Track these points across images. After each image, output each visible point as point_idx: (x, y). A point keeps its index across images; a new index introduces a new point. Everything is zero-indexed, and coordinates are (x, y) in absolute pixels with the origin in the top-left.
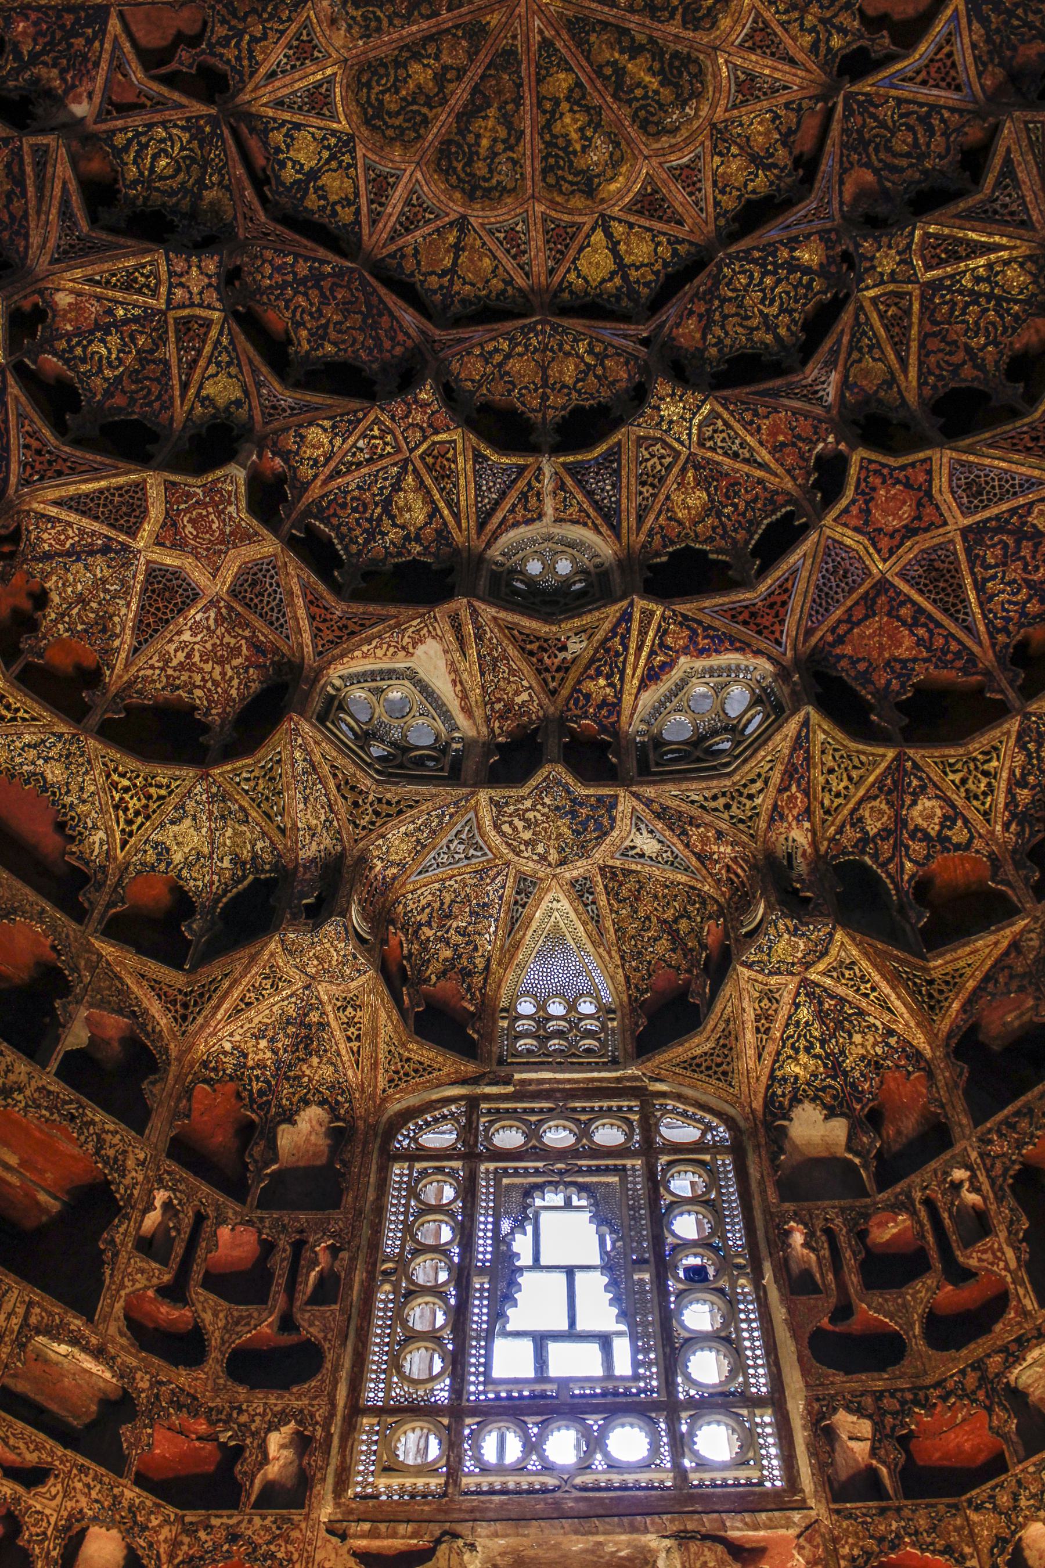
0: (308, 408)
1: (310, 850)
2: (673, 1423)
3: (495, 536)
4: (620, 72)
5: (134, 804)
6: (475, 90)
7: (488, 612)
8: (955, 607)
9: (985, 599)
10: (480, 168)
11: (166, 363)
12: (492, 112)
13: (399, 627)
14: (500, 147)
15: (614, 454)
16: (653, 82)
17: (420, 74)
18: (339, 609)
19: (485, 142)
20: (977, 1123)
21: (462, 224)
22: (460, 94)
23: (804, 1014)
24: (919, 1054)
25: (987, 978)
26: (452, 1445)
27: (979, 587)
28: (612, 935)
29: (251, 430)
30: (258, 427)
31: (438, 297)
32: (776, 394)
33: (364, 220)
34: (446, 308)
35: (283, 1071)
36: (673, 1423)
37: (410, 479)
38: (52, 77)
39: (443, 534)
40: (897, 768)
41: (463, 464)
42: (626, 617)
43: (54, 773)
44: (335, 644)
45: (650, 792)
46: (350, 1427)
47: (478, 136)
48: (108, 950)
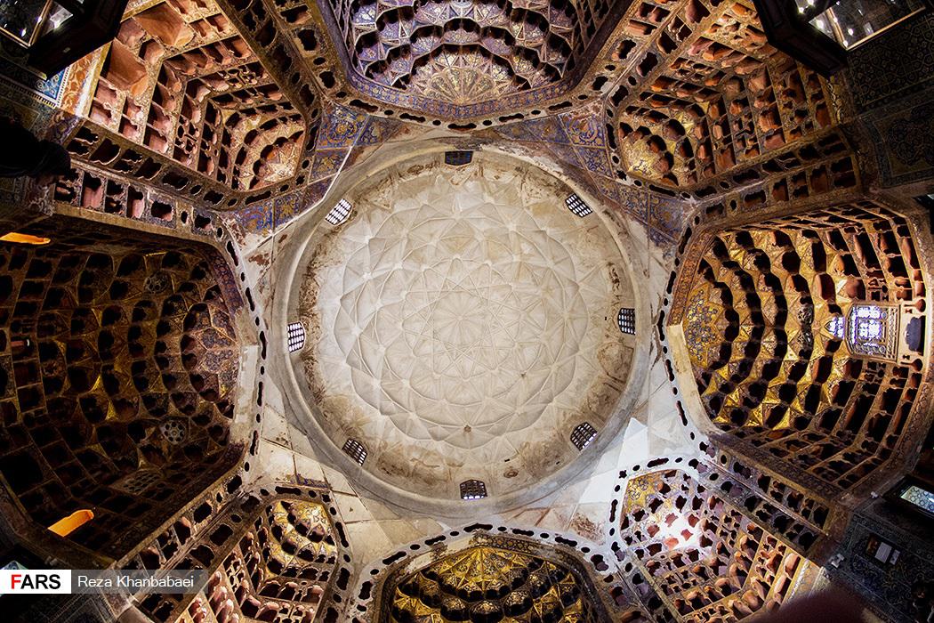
17: (480, 89)
22: (474, 87)
32: (422, 24)
38: (542, 78)
39: (480, 7)
41: (476, 16)
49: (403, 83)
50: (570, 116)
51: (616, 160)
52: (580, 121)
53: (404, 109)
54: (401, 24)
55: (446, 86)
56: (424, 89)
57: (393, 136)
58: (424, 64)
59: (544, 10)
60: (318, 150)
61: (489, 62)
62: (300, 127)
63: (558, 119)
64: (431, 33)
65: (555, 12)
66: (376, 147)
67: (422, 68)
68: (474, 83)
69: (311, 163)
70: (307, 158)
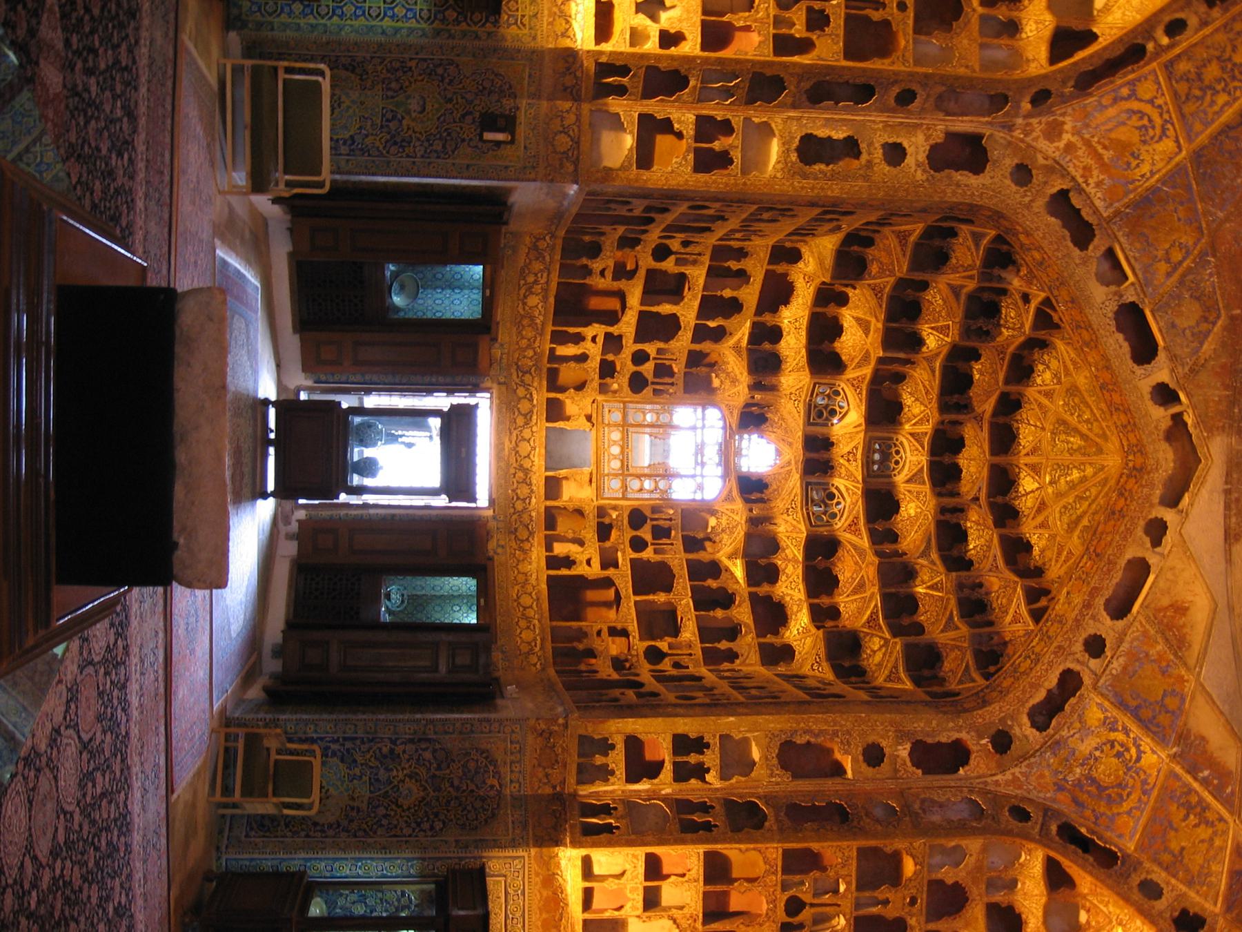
0: (933, 371)
1: (783, 380)
2: (621, 475)
3: (907, 439)
4: (1086, 499)
5: (797, 324)
6: (1087, 436)
7: (862, 435)
8: (855, 592)
9: (852, 601)
10: (1063, 437)
11: (938, 322)
12: (1083, 443)
13: (859, 406)
14: (1070, 445)
15: (924, 483)
16: (1078, 512)
18: (864, 387)
19: (1072, 439)
20: (687, 560)
21: (1043, 429)
22: (1084, 428)
23: (735, 524)
24: (718, 552)
25: (732, 574)
26: (616, 425)
27: (855, 600)
28: (782, 470)
29: (917, 353)
30: (919, 356)
31: (1019, 418)
32: (929, 540)
33: (1039, 388)
34: (1017, 421)
35: (728, 374)
36: (621, 475)
37: (923, 408)
38: (1024, 271)
39: (909, 420)
40: (796, 561)
42: (858, 482)
43: (800, 300)
44: (853, 385)
45: (798, 484)
46: (620, 402)
47: (1074, 437)
48: (748, 324)
49: (1043, 602)
50: (1099, 184)
51: (1176, 28)
52: (1107, 155)
53: (1088, 605)
54: (920, 590)
55: (1080, 498)
56: (1070, 552)
57: (1179, 644)
58: (1028, 547)
59: (877, 291)
60: (1131, 846)
61: (1031, 393)
62: (1033, 863)
63: (1117, 213)
64: (959, 525)
65: (874, 268)
66: (1200, 700)
67: (1036, 551)
68: (1077, 431)
69: (1159, 876)
70: (1135, 880)
